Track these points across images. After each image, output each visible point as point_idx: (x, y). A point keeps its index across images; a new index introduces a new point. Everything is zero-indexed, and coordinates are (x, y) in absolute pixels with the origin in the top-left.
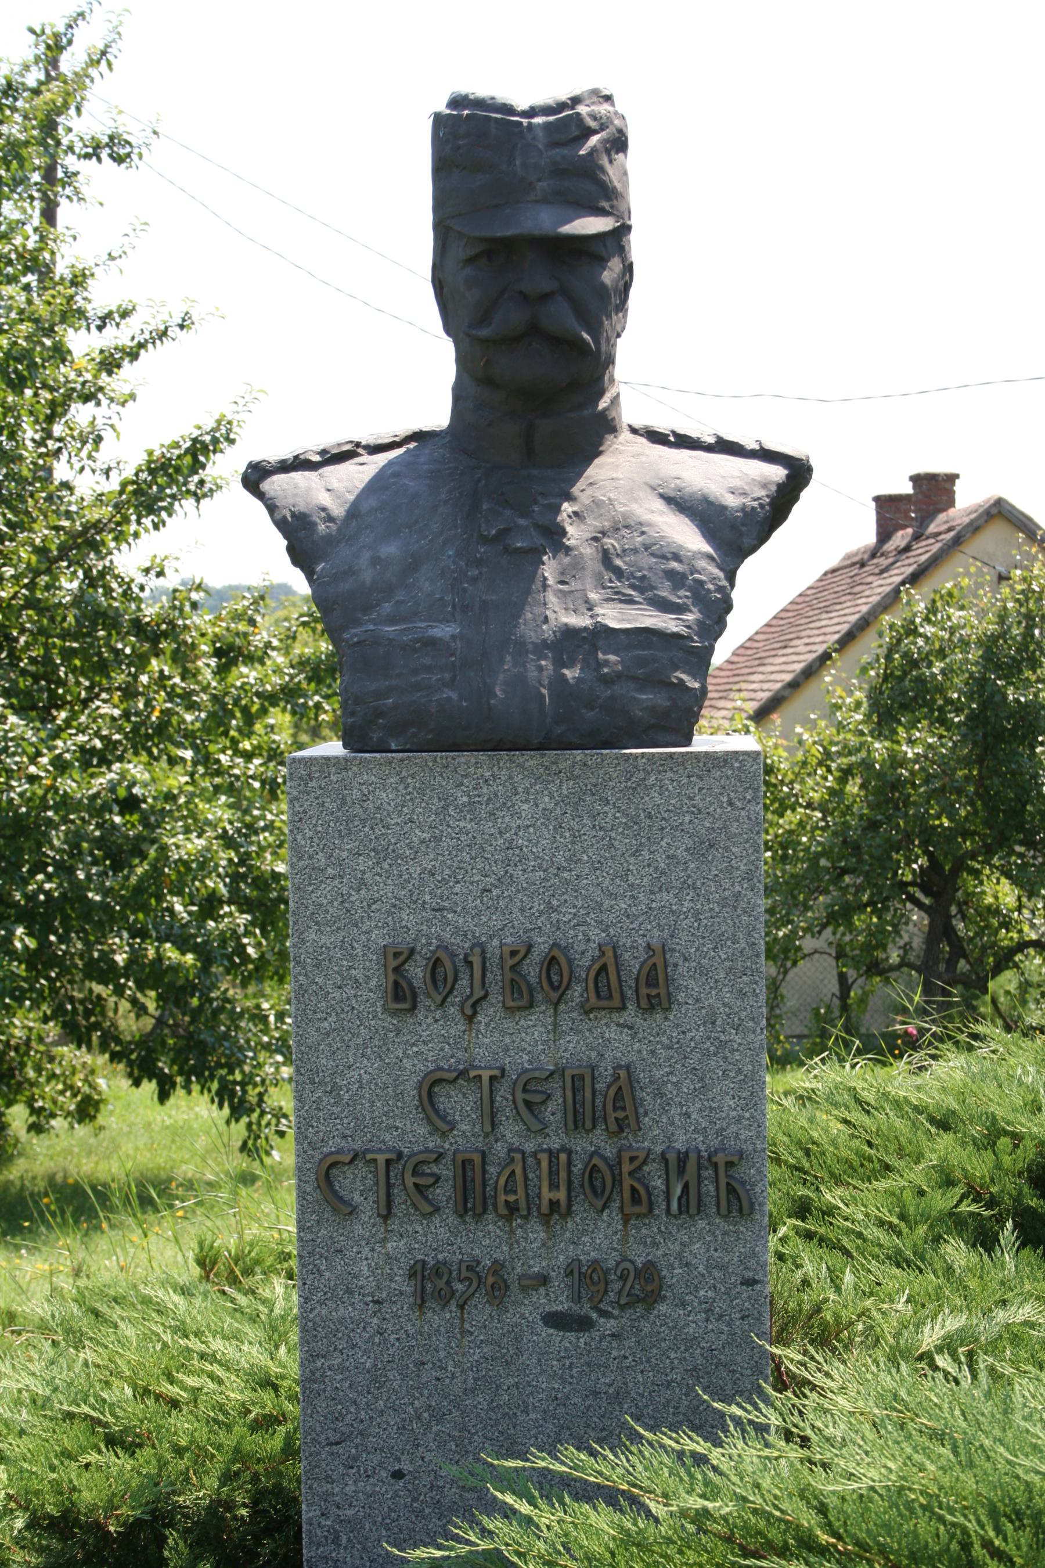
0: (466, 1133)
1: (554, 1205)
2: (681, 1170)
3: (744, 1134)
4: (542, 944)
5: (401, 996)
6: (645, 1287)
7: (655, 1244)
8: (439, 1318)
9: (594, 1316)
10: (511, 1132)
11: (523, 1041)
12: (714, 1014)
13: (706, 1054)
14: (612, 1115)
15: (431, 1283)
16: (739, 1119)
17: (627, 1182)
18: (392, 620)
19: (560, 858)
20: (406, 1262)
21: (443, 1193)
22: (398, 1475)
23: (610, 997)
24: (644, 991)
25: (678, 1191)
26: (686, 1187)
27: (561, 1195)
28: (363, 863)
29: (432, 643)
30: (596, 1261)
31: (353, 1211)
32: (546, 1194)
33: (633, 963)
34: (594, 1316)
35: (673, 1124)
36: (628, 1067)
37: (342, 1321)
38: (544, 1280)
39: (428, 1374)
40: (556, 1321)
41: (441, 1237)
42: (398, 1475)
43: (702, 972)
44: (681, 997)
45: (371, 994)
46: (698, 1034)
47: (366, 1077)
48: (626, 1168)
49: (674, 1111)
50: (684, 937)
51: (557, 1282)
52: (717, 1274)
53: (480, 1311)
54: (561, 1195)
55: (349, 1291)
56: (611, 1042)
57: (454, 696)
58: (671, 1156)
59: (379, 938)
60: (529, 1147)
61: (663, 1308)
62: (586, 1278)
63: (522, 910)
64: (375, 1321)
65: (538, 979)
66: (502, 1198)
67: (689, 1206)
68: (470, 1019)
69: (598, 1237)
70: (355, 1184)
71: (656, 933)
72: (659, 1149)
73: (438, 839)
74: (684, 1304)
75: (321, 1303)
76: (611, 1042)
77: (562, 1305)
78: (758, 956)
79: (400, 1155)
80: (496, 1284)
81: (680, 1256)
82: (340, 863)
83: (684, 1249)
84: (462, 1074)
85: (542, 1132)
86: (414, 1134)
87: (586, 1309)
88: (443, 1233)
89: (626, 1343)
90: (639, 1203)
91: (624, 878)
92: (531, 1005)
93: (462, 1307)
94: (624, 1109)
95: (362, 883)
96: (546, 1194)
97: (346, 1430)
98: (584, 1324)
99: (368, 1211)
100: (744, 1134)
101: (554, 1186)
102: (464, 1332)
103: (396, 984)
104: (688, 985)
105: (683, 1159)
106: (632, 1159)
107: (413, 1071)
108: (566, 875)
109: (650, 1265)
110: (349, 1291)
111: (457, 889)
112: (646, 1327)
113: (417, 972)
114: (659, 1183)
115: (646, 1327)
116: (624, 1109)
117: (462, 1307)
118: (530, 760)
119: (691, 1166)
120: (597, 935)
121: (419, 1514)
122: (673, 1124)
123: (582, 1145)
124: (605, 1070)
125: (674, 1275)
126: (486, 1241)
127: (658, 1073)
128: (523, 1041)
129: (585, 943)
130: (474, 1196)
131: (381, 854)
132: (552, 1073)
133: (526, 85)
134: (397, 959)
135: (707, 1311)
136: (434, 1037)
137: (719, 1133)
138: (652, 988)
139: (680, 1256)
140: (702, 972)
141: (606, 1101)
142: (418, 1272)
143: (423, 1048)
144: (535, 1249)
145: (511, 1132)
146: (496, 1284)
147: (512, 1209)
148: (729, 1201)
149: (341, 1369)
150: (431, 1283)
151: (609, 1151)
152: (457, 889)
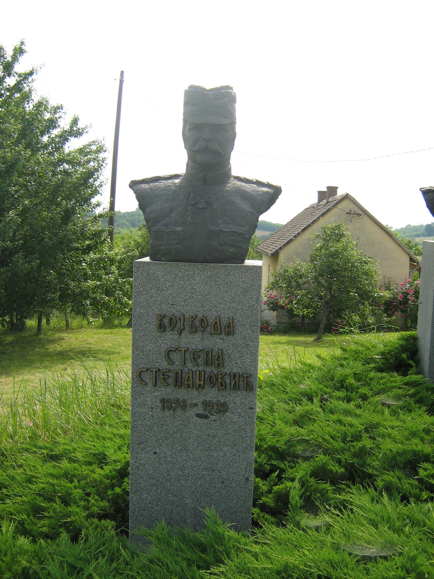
0: (177, 365)
1: (200, 385)
2: (234, 378)
3: (252, 369)
4: (200, 315)
5: (161, 327)
6: (223, 408)
7: (227, 397)
8: (168, 413)
9: (209, 415)
10: (189, 365)
11: (194, 341)
12: (245, 337)
14: (216, 362)
15: (166, 404)
16: (251, 365)
17: (220, 380)
19: (206, 292)
21: (171, 381)
22: (155, 453)
23: (218, 331)
24: (227, 329)
25: (233, 383)
26: (235, 382)
27: (202, 383)
28: (153, 291)
30: (210, 401)
31: (146, 384)
32: (198, 382)
33: (224, 322)
34: (209, 415)
35: (232, 366)
36: (221, 350)
37: (142, 412)
38: (196, 405)
39: (165, 427)
40: (199, 416)
41: (170, 392)
42: (155, 453)
44: (237, 332)
45: (153, 327)
46: (241, 342)
47: (151, 348)
48: (220, 376)
52: (243, 406)
53: (179, 412)
55: (144, 405)
56: (218, 343)
57: (180, 247)
58: (232, 374)
59: (156, 311)
60: (194, 369)
61: (228, 414)
62: (207, 404)
63: (195, 306)
64: (151, 413)
65: (198, 325)
66: (186, 383)
67: (236, 387)
68: (180, 334)
69: (212, 394)
70: (147, 377)
71: (231, 314)
72: (229, 372)
73: (173, 285)
74: (233, 413)
75: (137, 407)
76: (218, 343)
77: (201, 412)
78: (258, 322)
79: (159, 370)
80: (183, 405)
81: (233, 400)
82: (147, 290)
83: (234, 399)
84: (177, 349)
85: (198, 365)
86: (164, 365)
87: (207, 413)
89: (218, 423)
90: (223, 386)
91: (223, 299)
92: (196, 332)
93: (174, 411)
94: (220, 361)
95: (152, 297)
96: (198, 382)
97: (142, 441)
98: (206, 417)
99: (150, 384)
100: (252, 369)
101: (200, 380)
102: (174, 417)
103: (160, 324)
105: (235, 375)
106: (221, 374)
108: (207, 297)
110: (144, 405)
111: (178, 299)
112: (223, 419)
113: (166, 321)
115: (223, 419)
116: (220, 361)
117: (174, 411)
118: (199, 265)
119: (237, 377)
120: (215, 314)
121: (161, 464)
123: (208, 370)
124: (215, 350)
126: (181, 394)
128: (194, 341)
129: (212, 316)
130: (178, 382)
132: (201, 350)
134: (162, 318)
135: (239, 415)
136: (169, 339)
137: (245, 368)
138: (229, 329)
139: (233, 400)
141: (215, 359)
142: (163, 401)
143: (167, 341)
144: (194, 396)
145: (189, 365)
146: (183, 405)
147: (189, 386)
148: (247, 387)
151: (215, 372)
152: (178, 299)
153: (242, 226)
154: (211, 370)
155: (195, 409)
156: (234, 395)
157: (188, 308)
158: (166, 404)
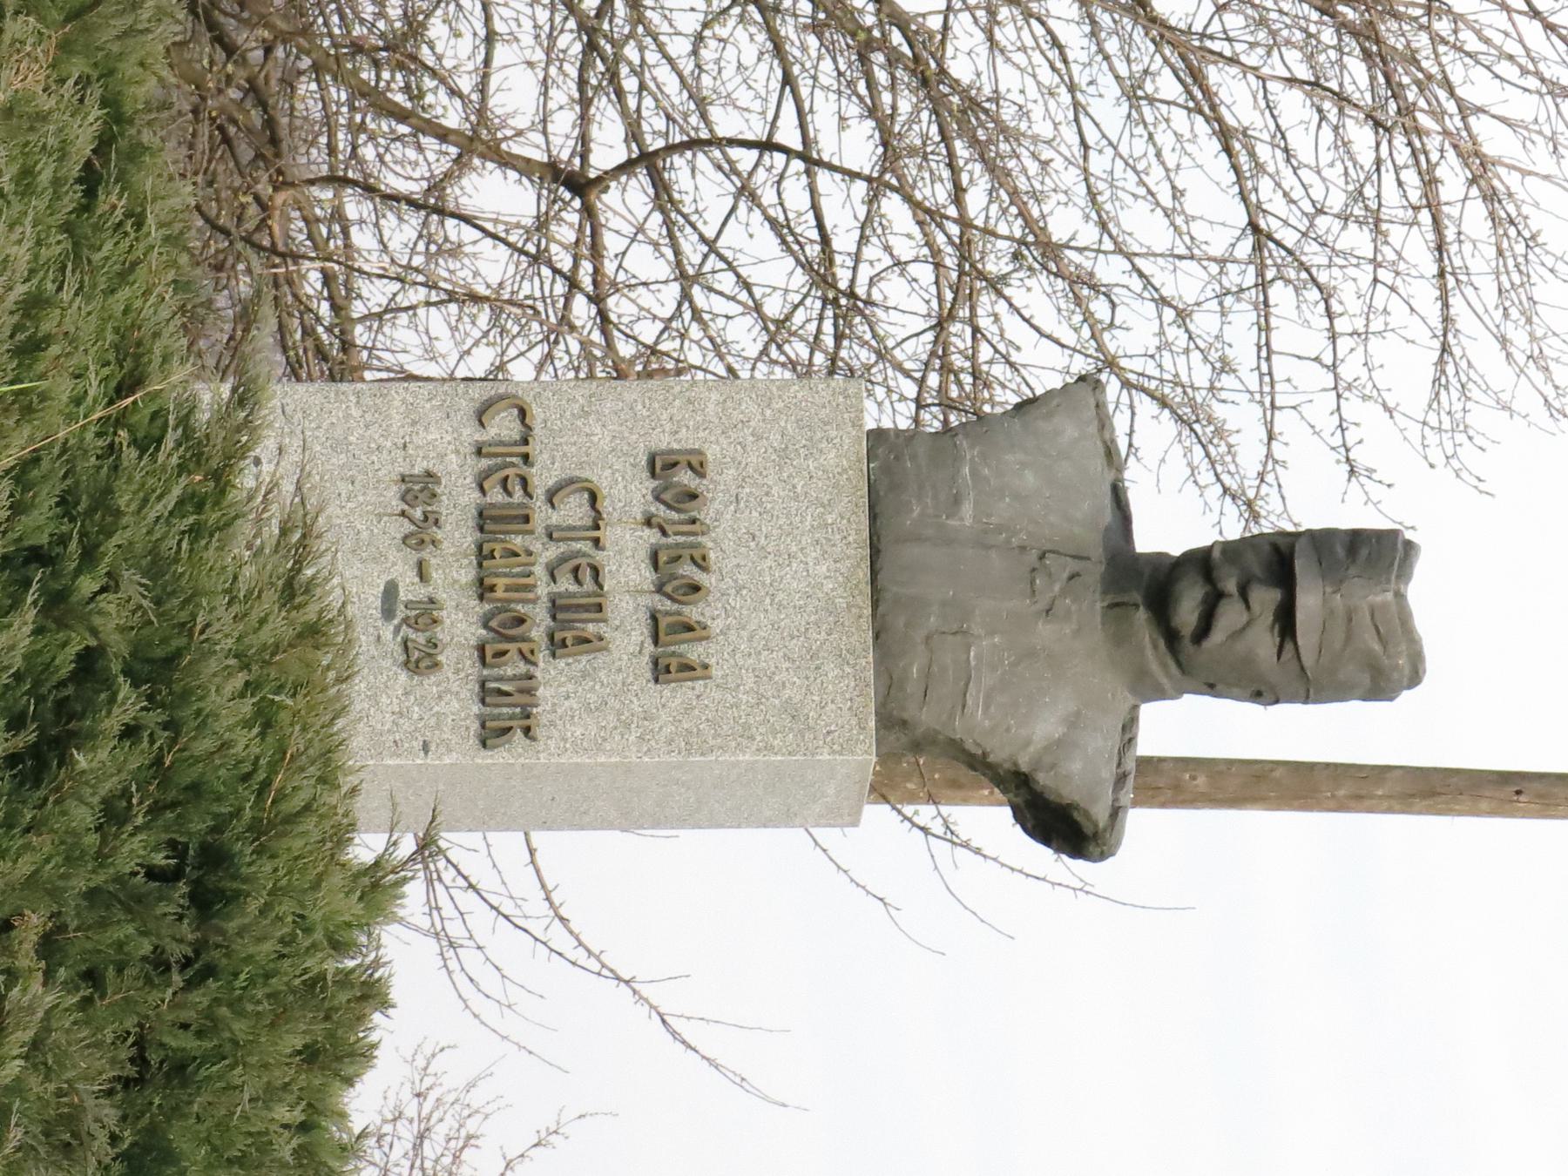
2: (521, 691)
7: (457, 672)
9: (396, 622)
12: (652, 719)
13: (619, 713)
14: (569, 635)
16: (565, 740)
18: (974, 473)
19: (781, 596)
20: (437, 469)
25: (505, 688)
26: (507, 694)
28: (775, 439)
29: (957, 501)
30: (442, 622)
33: (695, 652)
34: (396, 622)
35: (558, 684)
36: (606, 649)
37: (388, 417)
39: (344, 487)
40: (390, 591)
41: (459, 499)
43: (688, 710)
44: (667, 693)
45: (663, 441)
46: (636, 707)
47: (595, 439)
48: (525, 647)
49: (570, 687)
50: (717, 695)
51: (422, 592)
52: (433, 721)
54: (499, 593)
57: (915, 514)
58: (532, 683)
59: (712, 452)
61: (403, 677)
62: (426, 615)
63: (738, 566)
64: (389, 444)
69: (461, 625)
70: (503, 426)
71: (720, 673)
72: (538, 674)
73: (796, 498)
74: (406, 694)
75: (404, 401)
77: (403, 596)
78: (702, 754)
81: (448, 691)
82: (776, 420)
86: (543, 476)
87: (401, 612)
88: (464, 500)
89: (372, 648)
93: (403, 514)
95: (758, 437)
97: (295, 420)
98: (388, 612)
101: (508, 589)
102: (380, 516)
104: (677, 695)
105: (529, 692)
107: (602, 479)
108: (768, 601)
109: (436, 665)
110: (414, 423)
111: (755, 514)
112: (387, 663)
114: (510, 672)
115: (387, 663)
117: (403, 514)
118: (864, 573)
122: (558, 684)
124: (602, 628)
125: (430, 684)
126: (458, 535)
127: (602, 674)
131: (783, 454)
132: (601, 587)
133: (1425, 594)
135: (400, 713)
136: (629, 493)
137: (552, 723)
139: (448, 691)
140: (688, 710)
143: (621, 486)
144: (453, 572)
149: (348, 416)
150: (419, 490)
152: (755, 514)
153: (987, 707)
154: (539, 624)
155: (411, 576)
156: (465, 694)
157: (728, 545)
158: (419, 490)
